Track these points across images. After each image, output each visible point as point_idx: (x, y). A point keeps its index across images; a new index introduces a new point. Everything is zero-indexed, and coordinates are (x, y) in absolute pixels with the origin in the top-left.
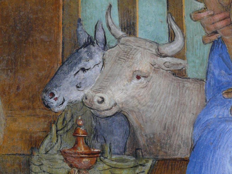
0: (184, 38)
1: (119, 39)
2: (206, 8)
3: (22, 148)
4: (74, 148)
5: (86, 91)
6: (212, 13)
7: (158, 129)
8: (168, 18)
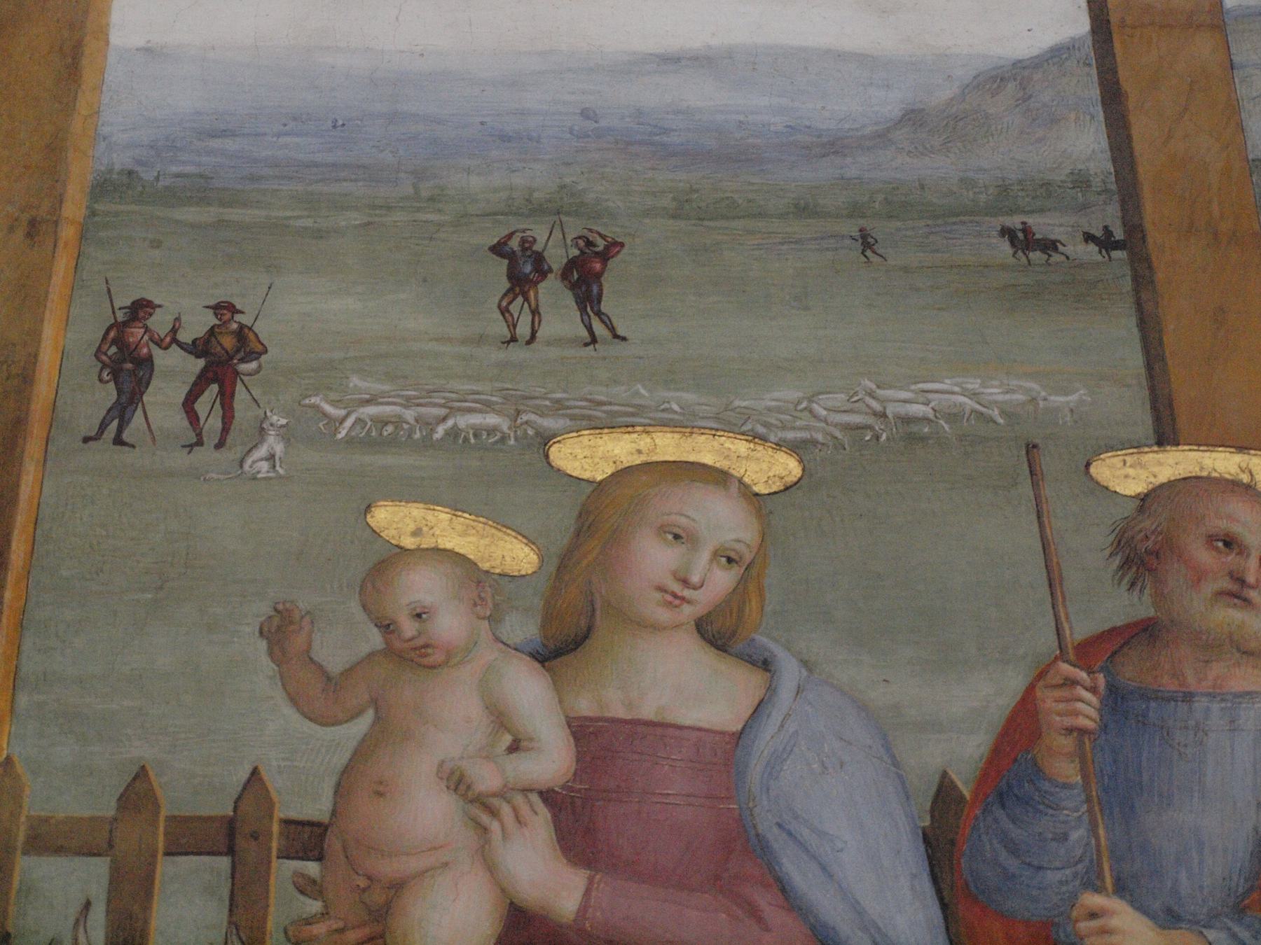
2: (327, 914)
6: (341, 924)
8: (229, 936)
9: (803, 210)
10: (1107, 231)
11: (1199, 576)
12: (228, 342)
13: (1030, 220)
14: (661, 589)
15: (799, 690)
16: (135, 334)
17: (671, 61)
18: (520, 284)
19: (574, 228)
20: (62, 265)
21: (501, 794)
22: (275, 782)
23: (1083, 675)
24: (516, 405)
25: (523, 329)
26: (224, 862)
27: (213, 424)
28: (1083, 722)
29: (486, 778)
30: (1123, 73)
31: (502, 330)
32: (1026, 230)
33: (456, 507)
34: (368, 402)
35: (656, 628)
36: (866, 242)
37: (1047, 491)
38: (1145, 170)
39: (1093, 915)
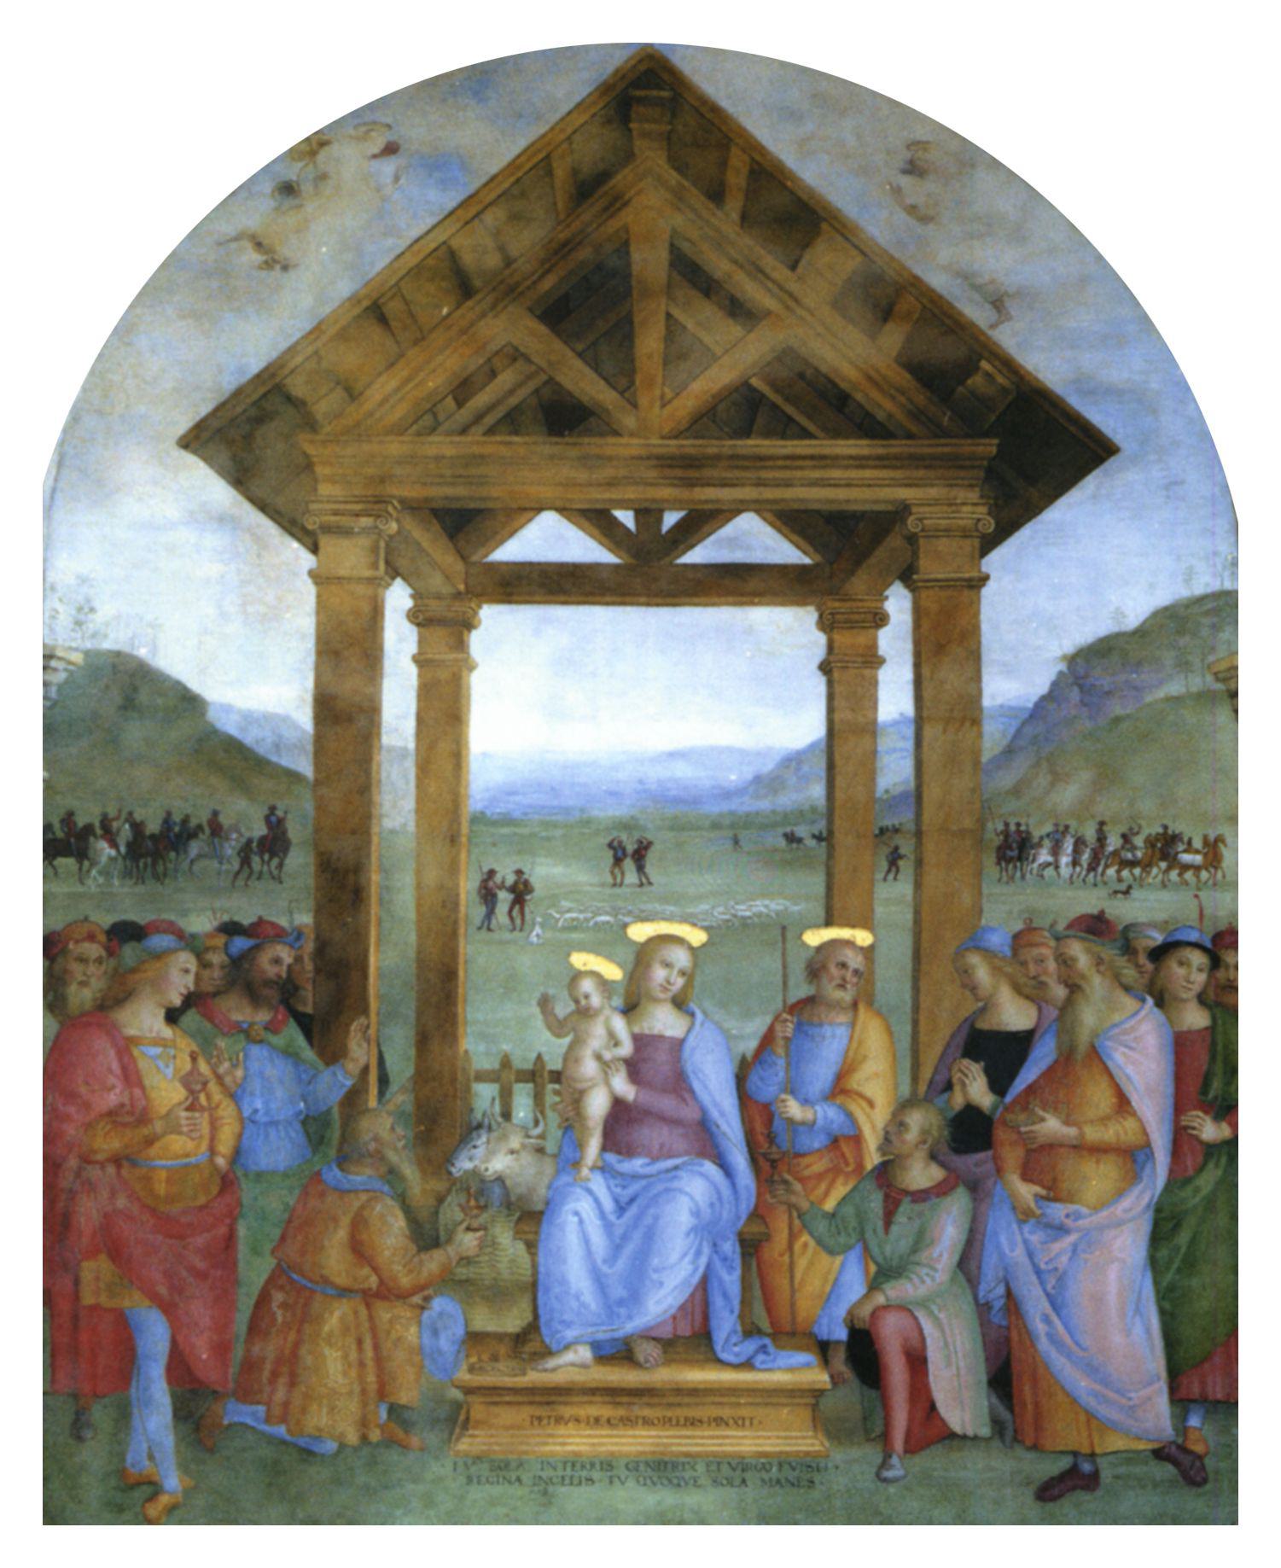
0: (546, 1125)
1: (499, 1124)
3: (432, 1201)
4: (468, 1201)
5: (477, 1162)
7: (521, 1190)
9: (716, 826)
10: (821, 833)
11: (831, 979)
12: (521, 887)
13: (795, 829)
14: (661, 985)
15: (702, 1024)
16: (491, 884)
17: (672, 755)
18: (618, 861)
19: (636, 835)
20: (463, 856)
21: (612, 1061)
22: (546, 1058)
23: (789, 1017)
24: (615, 911)
25: (619, 880)
26: (531, 1085)
27: (518, 922)
28: (789, 1035)
29: (607, 1055)
30: (837, 757)
31: (610, 880)
32: (792, 834)
33: (598, 953)
34: (569, 911)
35: (656, 1000)
36: (736, 841)
37: (789, 946)
38: (838, 803)
39: (783, 1101)
